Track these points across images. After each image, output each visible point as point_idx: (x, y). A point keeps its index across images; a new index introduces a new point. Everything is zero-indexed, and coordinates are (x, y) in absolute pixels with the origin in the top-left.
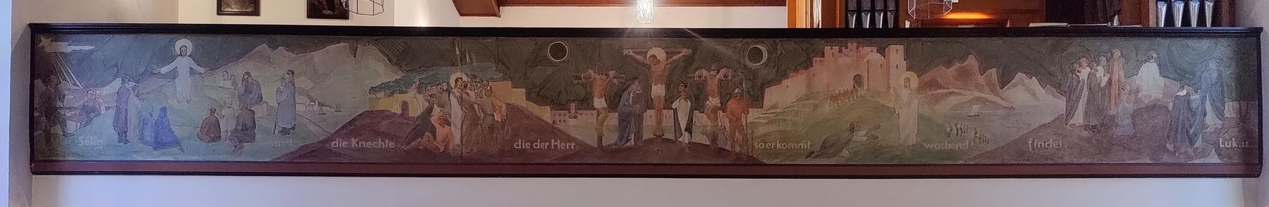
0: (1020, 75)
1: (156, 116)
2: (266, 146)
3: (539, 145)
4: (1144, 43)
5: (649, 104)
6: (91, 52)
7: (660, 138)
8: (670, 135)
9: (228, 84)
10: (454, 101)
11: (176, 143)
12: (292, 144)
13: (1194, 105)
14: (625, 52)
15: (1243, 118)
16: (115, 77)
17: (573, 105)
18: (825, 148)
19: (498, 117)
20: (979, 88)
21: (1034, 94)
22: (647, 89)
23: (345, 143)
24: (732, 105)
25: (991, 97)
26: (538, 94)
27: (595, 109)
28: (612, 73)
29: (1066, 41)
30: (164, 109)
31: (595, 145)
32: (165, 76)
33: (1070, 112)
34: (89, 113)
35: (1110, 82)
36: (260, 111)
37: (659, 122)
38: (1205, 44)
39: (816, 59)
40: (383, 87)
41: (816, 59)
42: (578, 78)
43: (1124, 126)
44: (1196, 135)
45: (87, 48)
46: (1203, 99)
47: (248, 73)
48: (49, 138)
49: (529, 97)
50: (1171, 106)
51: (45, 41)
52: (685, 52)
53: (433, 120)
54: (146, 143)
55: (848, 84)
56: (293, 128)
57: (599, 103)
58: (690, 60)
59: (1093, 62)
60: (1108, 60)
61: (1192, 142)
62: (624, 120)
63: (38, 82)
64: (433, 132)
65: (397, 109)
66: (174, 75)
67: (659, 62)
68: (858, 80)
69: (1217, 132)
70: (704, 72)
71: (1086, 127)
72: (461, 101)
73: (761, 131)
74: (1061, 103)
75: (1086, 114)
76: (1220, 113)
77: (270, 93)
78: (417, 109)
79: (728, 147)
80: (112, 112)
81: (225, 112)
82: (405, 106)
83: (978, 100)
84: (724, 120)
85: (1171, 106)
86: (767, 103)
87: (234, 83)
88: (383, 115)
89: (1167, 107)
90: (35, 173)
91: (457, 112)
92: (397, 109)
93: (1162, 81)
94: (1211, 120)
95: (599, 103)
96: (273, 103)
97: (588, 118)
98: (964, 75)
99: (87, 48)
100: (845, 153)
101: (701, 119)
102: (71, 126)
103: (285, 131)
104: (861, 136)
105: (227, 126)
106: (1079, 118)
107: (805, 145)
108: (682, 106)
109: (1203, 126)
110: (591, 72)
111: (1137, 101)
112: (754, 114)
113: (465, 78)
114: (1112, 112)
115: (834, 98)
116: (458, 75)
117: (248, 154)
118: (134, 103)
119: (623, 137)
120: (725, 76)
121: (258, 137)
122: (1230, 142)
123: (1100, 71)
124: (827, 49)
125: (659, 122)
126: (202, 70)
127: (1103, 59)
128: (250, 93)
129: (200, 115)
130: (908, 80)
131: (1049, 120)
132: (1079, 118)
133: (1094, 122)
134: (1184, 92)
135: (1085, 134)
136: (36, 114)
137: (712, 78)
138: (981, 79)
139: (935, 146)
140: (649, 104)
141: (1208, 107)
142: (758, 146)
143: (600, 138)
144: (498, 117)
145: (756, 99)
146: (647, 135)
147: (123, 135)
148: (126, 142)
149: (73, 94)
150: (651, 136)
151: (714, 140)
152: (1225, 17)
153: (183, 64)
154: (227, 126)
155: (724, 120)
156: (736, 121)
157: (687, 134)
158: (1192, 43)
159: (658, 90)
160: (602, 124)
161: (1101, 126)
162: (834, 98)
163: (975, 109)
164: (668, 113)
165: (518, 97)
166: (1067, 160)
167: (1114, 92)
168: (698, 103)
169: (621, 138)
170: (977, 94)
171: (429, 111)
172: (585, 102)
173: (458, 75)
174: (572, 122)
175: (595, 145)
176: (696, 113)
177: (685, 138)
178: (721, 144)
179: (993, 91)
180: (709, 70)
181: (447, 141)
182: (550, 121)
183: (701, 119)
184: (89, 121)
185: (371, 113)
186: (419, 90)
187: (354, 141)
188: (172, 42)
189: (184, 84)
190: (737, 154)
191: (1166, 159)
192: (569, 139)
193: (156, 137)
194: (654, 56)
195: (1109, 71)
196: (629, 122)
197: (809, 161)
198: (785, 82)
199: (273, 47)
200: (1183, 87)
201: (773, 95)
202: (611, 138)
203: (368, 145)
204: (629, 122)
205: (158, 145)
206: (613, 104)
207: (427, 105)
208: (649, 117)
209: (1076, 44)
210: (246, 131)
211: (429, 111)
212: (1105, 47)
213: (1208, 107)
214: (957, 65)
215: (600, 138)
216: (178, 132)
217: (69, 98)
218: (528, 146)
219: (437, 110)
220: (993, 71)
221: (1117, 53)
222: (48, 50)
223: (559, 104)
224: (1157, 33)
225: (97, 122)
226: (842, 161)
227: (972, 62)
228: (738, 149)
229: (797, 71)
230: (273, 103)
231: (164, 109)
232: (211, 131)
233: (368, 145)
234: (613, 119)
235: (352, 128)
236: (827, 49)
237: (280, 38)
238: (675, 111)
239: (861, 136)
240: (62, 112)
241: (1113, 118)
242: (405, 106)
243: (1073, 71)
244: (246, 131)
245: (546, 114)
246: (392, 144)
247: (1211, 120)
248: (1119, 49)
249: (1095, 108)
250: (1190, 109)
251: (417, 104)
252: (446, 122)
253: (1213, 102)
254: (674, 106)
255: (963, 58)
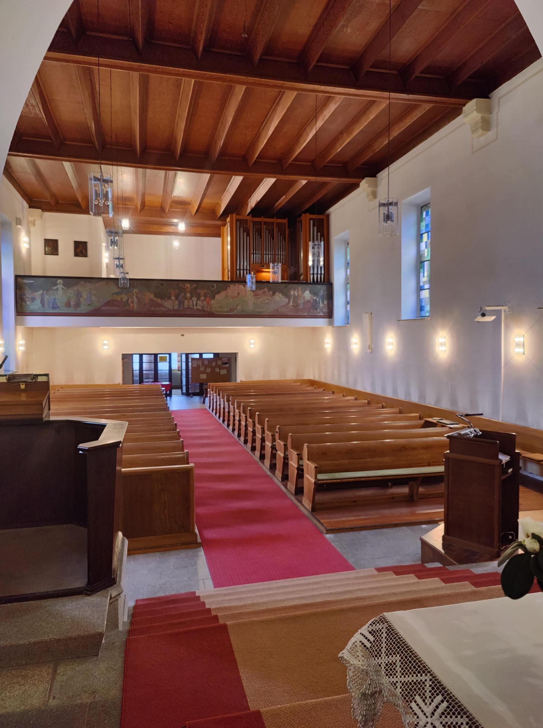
0: (277, 293)
1: (53, 300)
2: (83, 308)
3: (158, 309)
4: (306, 286)
5: (186, 299)
6: (33, 282)
7: (189, 307)
8: (192, 307)
9: (73, 292)
10: (135, 297)
11: (59, 308)
12: (91, 308)
13: (317, 301)
14: (180, 285)
15: (328, 304)
16: (41, 289)
17: (166, 299)
18: (231, 310)
19: (146, 302)
20: (268, 296)
21: (280, 298)
22: (186, 294)
23: (105, 308)
24: (207, 299)
25: (270, 298)
26: (157, 296)
27: (172, 300)
28: (176, 290)
29: (288, 285)
30: (55, 299)
31: (172, 308)
32: (55, 290)
33: (289, 302)
34: (33, 299)
35: (298, 295)
36: (82, 300)
37: (189, 303)
38: (320, 286)
39: (228, 288)
40: (116, 293)
41: (228, 288)
42: (167, 291)
43: (301, 306)
44: (318, 308)
45: (32, 281)
46: (319, 300)
47: (78, 289)
48: (21, 306)
49: (155, 296)
50: (312, 301)
51: (19, 280)
52: (195, 285)
53: (129, 302)
54: (50, 308)
55: (236, 294)
56: (91, 304)
57: (173, 298)
58: (196, 288)
59: (294, 290)
60: (298, 290)
61: (317, 310)
62: (179, 302)
63: (18, 291)
64: (129, 305)
65: (119, 299)
66: (57, 289)
67: (188, 288)
68: (238, 293)
69: (323, 308)
70: (200, 291)
71: (293, 306)
72: (137, 297)
73: (215, 306)
74: (287, 300)
75: (293, 303)
76: (323, 303)
77: (85, 295)
78: (125, 299)
79: (206, 310)
80: (40, 299)
81: (72, 299)
82: (121, 298)
83: (268, 299)
84: (205, 303)
85: (312, 301)
86: (216, 299)
87: (74, 292)
88: (116, 300)
89: (311, 301)
90: (17, 315)
91: (135, 300)
92: (119, 299)
93: (310, 295)
94: (321, 305)
95: (173, 298)
96: (85, 297)
97: (170, 302)
98: (264, 293)
99: (32, 281)
100: (235, 311)
101: (199, 302)
102: (28, 303)
103: (89, 305)
104: (239, 308)
105: (72, 303)
106: (291, 304)
107: (225, 309)
108: (195, 299)
109: (319, 306)
110: (171, 290)
111: (305, 300)
112: (213, 302)
113: (138, 291)
114: (299, 303)
115: (233, 298)
116: (136, 290)
117: (78, 311)
118: (46, 297)
119: (179, 307)
120: (205, 292)
121: (81, 306)
122: (325, 310)
123: (296, 292)
124: (231, 285)
125: (189, 303)
126: (65, 288)
127: (296, 290)
128: (79, 295)
129: (65, 300)
130: (251, 294)
131: (284, 304)
132: (291, 304)
133: (294, 305)
134: (315, 298)
135: (293, 308)
136: (17, 299)
137: (202, 292)
138: (268, 294)
139: (257, 310)
140: (186, 299)
141: (321, 302)
142: (214, 310)
143: (173, 307)
144: (146, 302)
145: (213, 298)
146: (186, 307)
147: (43, 305)
148: (44, 307)
149: (28, 294)
150: (187, 307)
151: (203, 308)
152: (326, 280)
153: (60, 287)
154: (72, 303)
155: (205, 303)
156: (208, 303)
157: (196, 306)
158: (317, 286)
159: (188, 295)
160: (174, 303)
161: (296, 306)
162: (233, 298)
163: (267, 301)
164: (191, 301)
165: (152, 296)
166: (288, 314)
167: (299, 297)
168: (199, 299)
169: (179, 307)
170: (267, 297)
171: (128, 300)
172: (169, 298)
173: (136, 290)
174: (166, 303)
175: (172, 308)
176: (198, 301)
177: (195, 307)
178: (204, 309)
179: (271, 297)
180: (201, 290)
181: (133, 307)
182: (160, 303)
183: (199, 302)
184: (33, 302)
185: (112, 300)
186: (125, 294)
187: (108, 307)
188: (57, 280)
189: (60, 292)
190: (209, 312)
191: (311, 314)
192: (166, 307)
193: (53, 306)
194: (187, 286)
195: (298, 292)
196: (181, 303)
197: (226, 314)
198: (220, 293)
199: (85, 282)
200: (315, 297)
201: (217, 296)
202: (176, 307)
203: (112, 308)
204: (181, 303)
205: (53, 308)
206: (177, 298)
207: (127, 298)
208: (186, 302)
209: (290, 286)
210: (78, 305)
211: (128, 300)
212: (297, 287)
213: (321, 302)
214: (262, 290)
215: (173, 307)
216: (59, 304)
217: (27, 295)
218: (154, 309)
219: (130, 300)
220: (271, 292)
221: (300, 288)
222: (20, 282)
223: (163, 299)
224: (310, 284)
225: (35, 302)
226: (235, 314)
227: (266, 289)
228: (209, 310)
229: (223, 291)
230: (85, 297)
231: (55, 299)
232: (68, 304)
233: (112, 308)
234: (177, 302)
235: (107, 304)
236: (231, 285)
237: (87, 280)
238: (193, 300)
239: (239, 308)
240: (25, 299)
241: (299, 304)
242: (121, 298)
243: (289, 292)
244: (78, 305)
245: (159, 301)
246: (118, 308)
247: (321, 305)
248: (300, 287)
249: (295, 301)
250: (316, 302)
251: (125, 298)
252: (133, 302)
253: (322, 300)
254: (192, 299)
255: (264, 289)
